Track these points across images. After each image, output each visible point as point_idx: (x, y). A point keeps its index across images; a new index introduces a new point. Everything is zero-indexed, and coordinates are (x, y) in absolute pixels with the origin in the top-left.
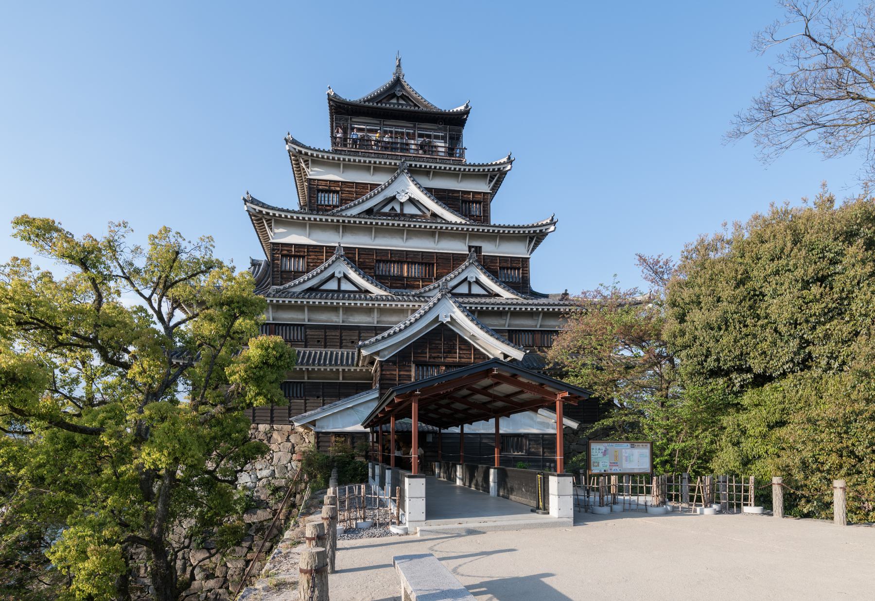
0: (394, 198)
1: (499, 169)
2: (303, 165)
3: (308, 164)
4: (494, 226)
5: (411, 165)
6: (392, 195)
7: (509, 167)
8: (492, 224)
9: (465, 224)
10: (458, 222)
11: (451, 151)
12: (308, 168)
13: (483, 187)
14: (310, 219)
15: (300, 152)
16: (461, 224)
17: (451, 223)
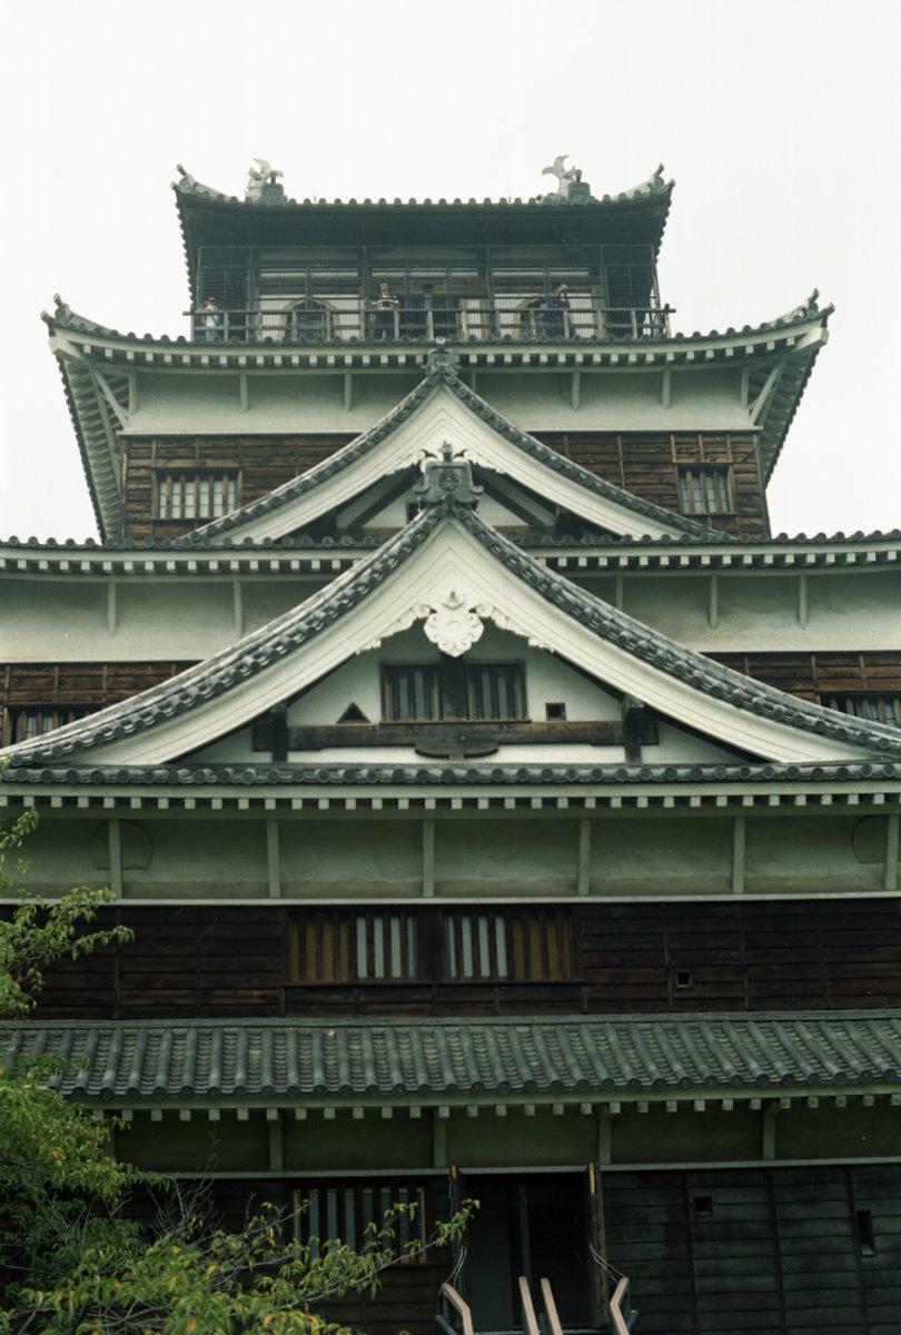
0: (411, 475)
1: (781, 344)
2: (110, 396)
3: (126, 393)
4: (783, 540)
5: (464, 360)
6: (406, 465)
7: (814, 334)
8: (775, 534)
9: (665, 543)
10: (637, 538)
11: (618, 328)
12: (125, 405)
13: (731, 416)
14: (118, 567)
15: (98, 354)
16: (646, 542)
17: (614, 540)
